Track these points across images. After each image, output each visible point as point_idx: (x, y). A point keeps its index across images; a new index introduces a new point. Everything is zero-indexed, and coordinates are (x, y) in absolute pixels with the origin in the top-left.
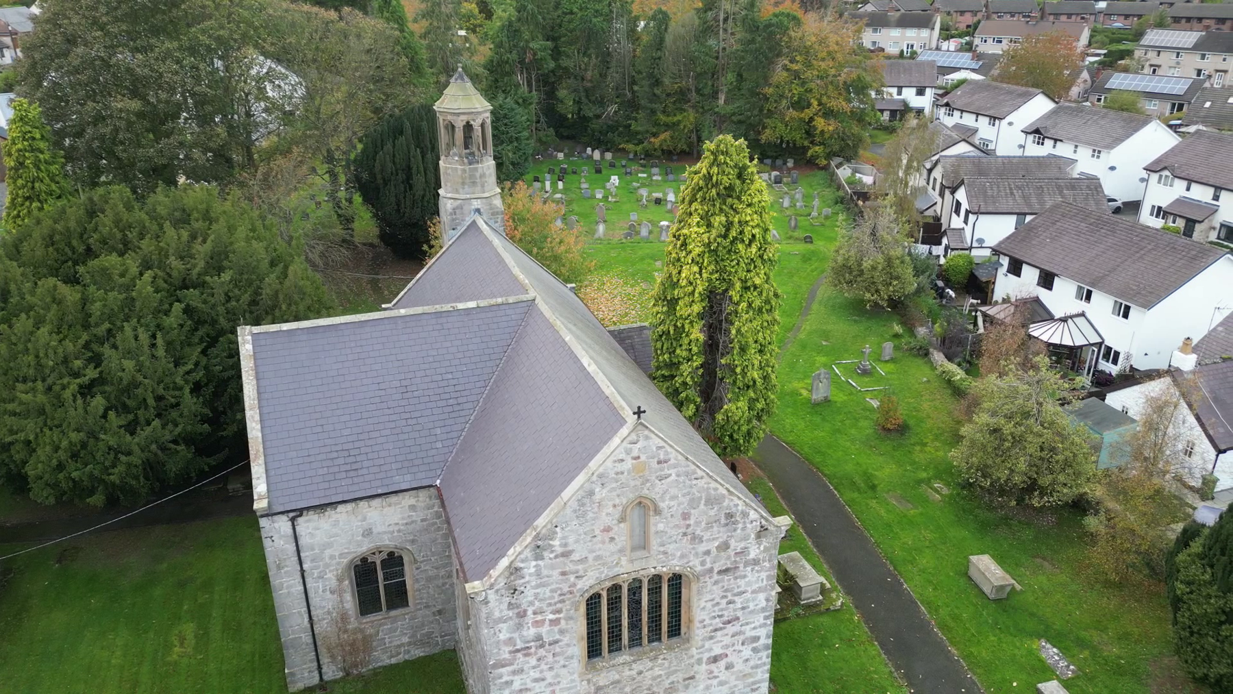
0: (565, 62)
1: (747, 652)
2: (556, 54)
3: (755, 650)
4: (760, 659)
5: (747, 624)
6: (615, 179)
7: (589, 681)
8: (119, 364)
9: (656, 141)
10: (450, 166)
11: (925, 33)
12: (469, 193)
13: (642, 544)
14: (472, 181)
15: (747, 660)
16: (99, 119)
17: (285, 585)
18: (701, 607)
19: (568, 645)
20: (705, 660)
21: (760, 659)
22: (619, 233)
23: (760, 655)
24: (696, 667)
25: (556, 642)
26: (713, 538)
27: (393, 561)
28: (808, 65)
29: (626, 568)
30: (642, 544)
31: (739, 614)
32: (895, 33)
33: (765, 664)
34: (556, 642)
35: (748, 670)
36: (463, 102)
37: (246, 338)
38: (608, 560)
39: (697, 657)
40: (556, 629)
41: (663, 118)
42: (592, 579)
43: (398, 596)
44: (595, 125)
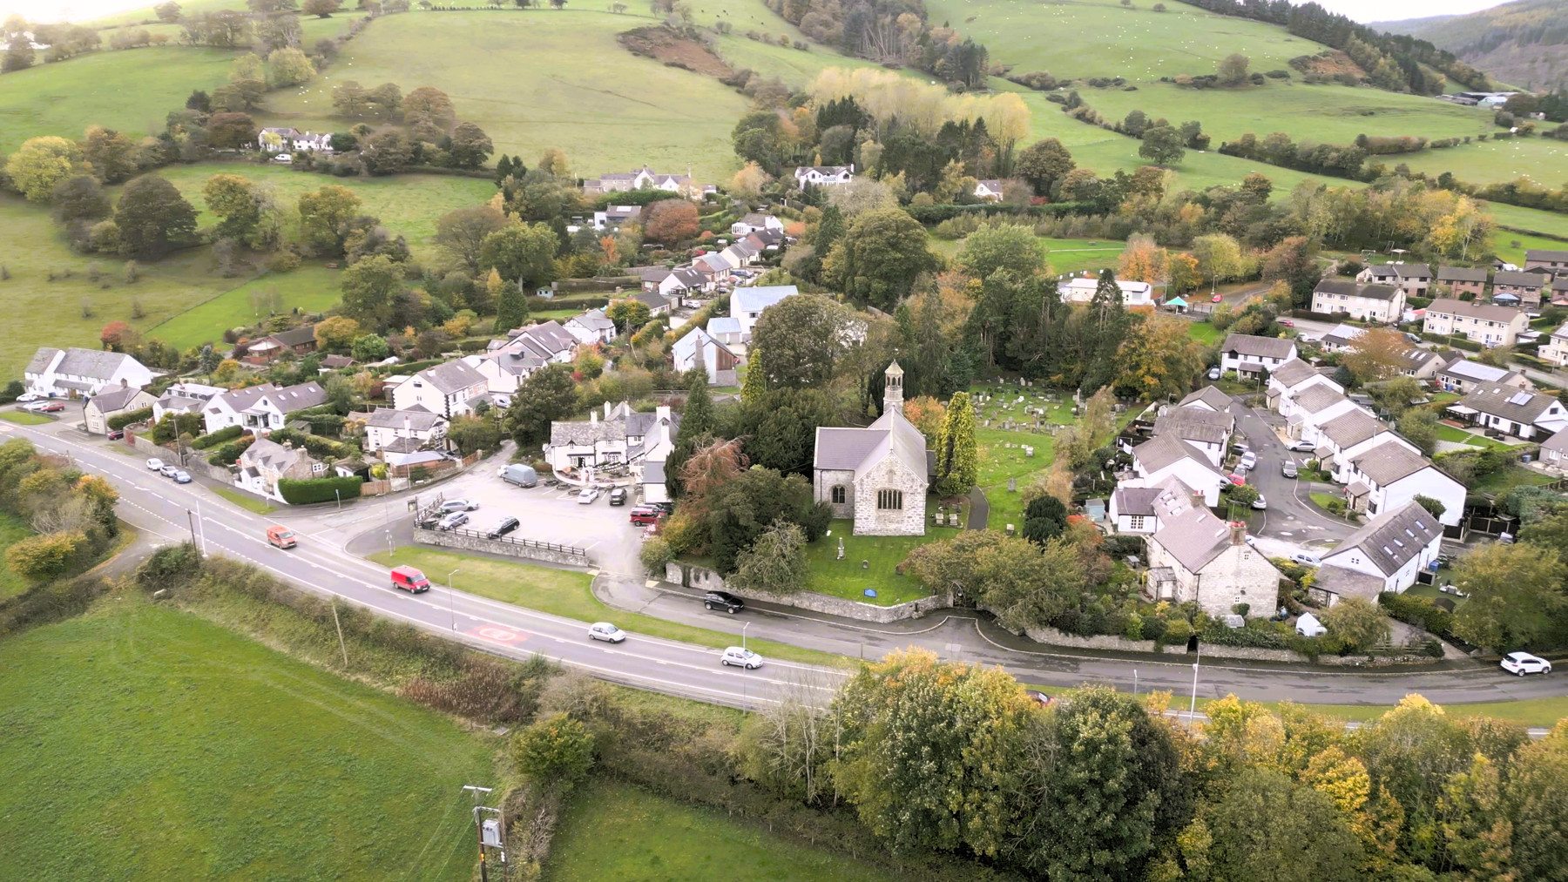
0: (1011, 328)
2: (1007, 323)
6: (1021, 399)
8: (787, 435)
9: (1054, 378)
10: (888, 390)
11: (1385, 303)
12: (893, 398)
13: (891, 481)
14: (892, 396)
16: (780, 356)
17: (817, 488)
18: (906, 501)
22: (994, 426)
26: (909, 484)
27: (842, 490)
28: (1143, 345)
29: (887, 486)
30: (891, 481)
32: (1360, 301)
36: (894, 371)
37: (818, 429)
38: (883, 484)
41: (1063, 365)
42: (879, 487)
43: (843, 501)
44: (1026, 365)
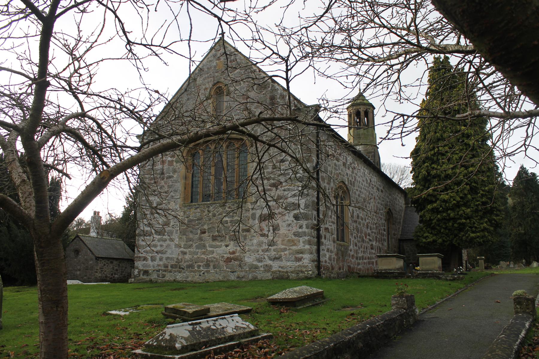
1: (289, 217)
3: (296, 217)
4: (301, 227)
5: (289, 190)
7: (185, 212)
15: (289, 225)
19: (176, 181)
20: (257, 216)
21: (301, 227)
23: (301, 222)
24: (251, 221)
25: (170, 177)
31: (282, 179)
33: (304, 234)
34: (170, 177)
35: (292, 237)
39: (251, 212)
40: (171, 168)
